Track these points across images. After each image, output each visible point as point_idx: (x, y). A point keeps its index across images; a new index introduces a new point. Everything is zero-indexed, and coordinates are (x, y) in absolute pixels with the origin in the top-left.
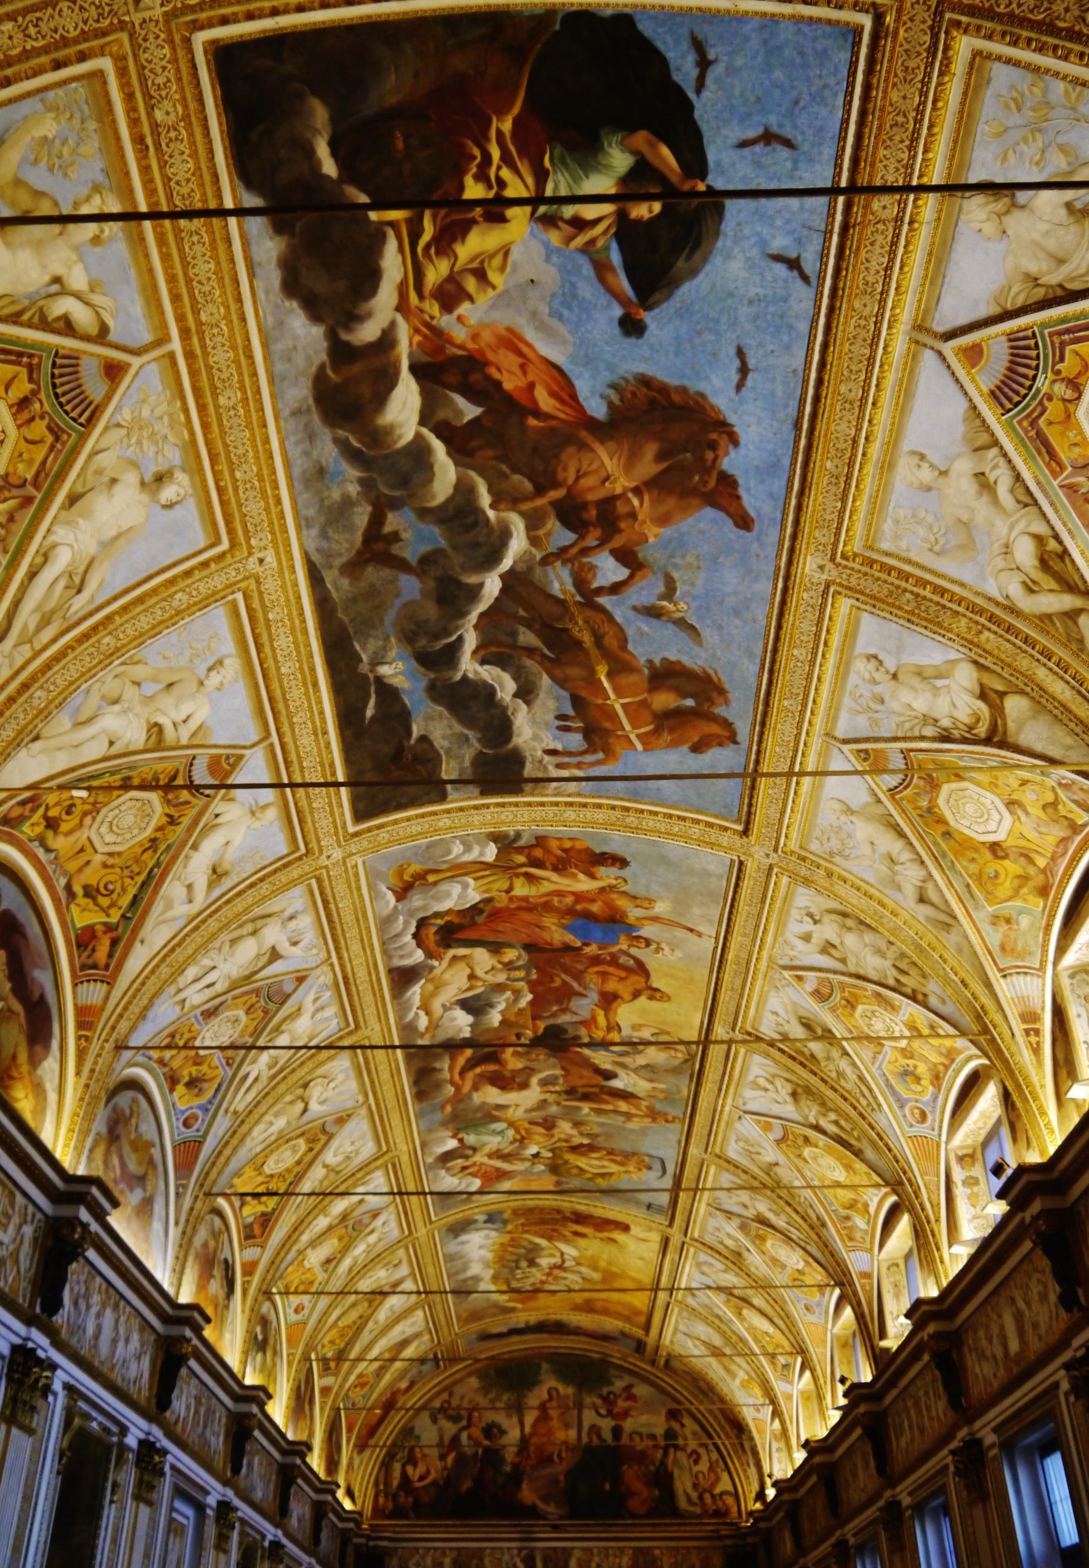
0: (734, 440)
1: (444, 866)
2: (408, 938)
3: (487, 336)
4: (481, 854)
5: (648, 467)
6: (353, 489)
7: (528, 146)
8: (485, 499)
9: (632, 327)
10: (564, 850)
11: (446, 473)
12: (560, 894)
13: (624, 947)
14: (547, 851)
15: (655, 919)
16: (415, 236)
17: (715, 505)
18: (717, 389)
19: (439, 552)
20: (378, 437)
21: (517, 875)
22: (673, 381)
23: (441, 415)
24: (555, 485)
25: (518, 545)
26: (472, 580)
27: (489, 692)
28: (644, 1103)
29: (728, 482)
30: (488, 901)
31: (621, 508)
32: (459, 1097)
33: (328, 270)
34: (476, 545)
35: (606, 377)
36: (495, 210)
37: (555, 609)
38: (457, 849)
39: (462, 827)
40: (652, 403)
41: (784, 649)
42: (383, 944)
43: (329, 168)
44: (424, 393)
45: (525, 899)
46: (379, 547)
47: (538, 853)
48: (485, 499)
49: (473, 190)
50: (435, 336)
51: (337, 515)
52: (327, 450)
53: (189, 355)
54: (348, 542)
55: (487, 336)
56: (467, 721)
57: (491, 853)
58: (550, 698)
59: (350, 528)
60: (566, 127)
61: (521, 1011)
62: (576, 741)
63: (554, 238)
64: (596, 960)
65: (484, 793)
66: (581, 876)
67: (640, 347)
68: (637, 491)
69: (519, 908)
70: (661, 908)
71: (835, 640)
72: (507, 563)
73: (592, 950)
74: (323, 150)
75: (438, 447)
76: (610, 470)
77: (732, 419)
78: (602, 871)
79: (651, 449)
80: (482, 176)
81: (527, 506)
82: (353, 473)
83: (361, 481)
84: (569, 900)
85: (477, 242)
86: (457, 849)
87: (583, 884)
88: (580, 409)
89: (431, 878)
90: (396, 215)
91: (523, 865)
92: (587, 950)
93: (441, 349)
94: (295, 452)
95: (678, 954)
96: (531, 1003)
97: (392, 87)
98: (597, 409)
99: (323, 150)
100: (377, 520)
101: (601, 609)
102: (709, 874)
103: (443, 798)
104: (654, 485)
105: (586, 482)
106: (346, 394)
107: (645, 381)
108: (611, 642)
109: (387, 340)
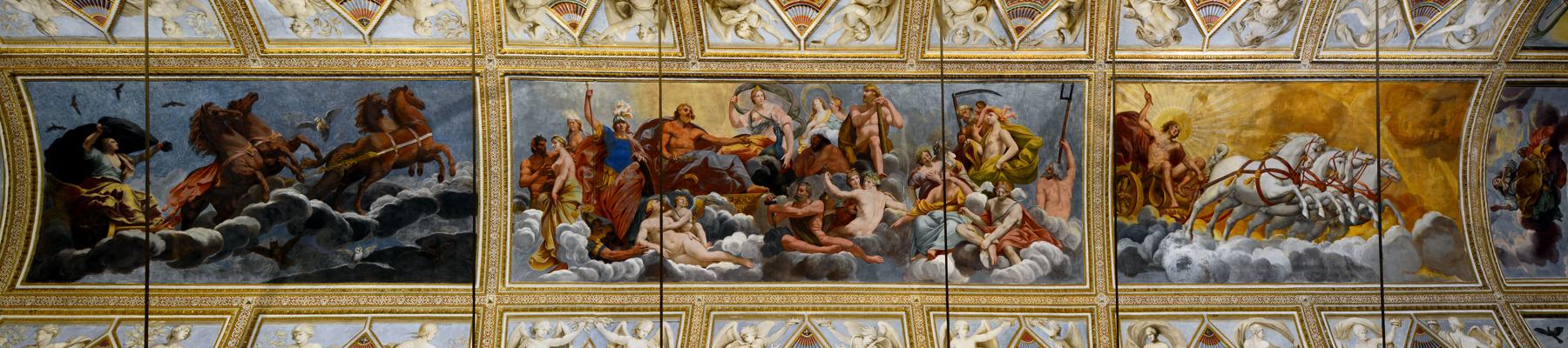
0: (210, 104)
1: (542, 239)
2: (609, 266)
3: (174, 200)
4: (534, 217)
5: (237, 138)
6: (239, 258)
7: (93, 184)
8: (262, 204)
9: (167, 147)
10: (533, 172)
11: (242, 220)
12: (579, 176)
13: (631, 137)
14: (534, 181)
15: (590, 120)
16: (123, 224)
17: (249, 110)
18: (187, 113)
19: (289, 226)
20: (214, 245)
21: (560, 199)
22: (189, 131)
23: (210, 220)
24: (255, 175)
25: (291, 192)
26: (310, 212)
27: (389, 211)
28: (855, 113)
29: (232, 105)
30: (586, 216)
31: (265, 148)
32: (863, 247)
33: (127, 257)
34: (289, 210)
35: (193, 156)
36: (119, 195)
37: (332, 177)
38: (526, 230)
39: (498, 226)
40: (202, 138)
41: (314, 71)
42: (603, 282)
43: (86, 251)
44: (197, 226)
45: (586, 196)
46: (277, 252)
47: (536, 186)
48: (262, 204)
49: (111, 202)
50: (169, 220)
51: (249, 271)
52: (213, 266)
53: (124, 313)
54: (270, 265)
55: (174, 200)
56: (411, 220)
57: (534, 215)
58: (400, 179)
59: (259, 263)
60: (89, 172)
61: (732, 200)
62: (426, 166)
63: (130, 175)
64: (654, 152)
65: (475, 212)
66: (558, 162)
67: (175, 143)
68: (253, 142)
69: (598, 198)
70: (573, 115)
71: (294, 48)
72: (302, 196)
73: (641, 156)
74: (79, 252)
75: (226, 222)
76: (243, 154)
77: (199, 106)
78: (550, 152)
79: (227, 137)
80: (103, 200)
81: (267, 188)
82: (230, 257)
83: (236, 255)
84: (584, 169)
85: (130, 203)
86: (526, 230)
87: (567, 161)
88: (211, 166)
89: (551, 246)
90: (112, 230)
91: (550, 195)
92: (640, 158)
93: (177, 219)
94: (205, 279)
95: (622, 103)
96: (721, 193)
97: (63, 227)
98: (210, 159)
99: (79, 252)
100: (262, 251)
101: (330, 156)
102: (532, 92)
103: (474, 236)
104: (248, 134)
105: (252, 162)
106: (186, 257)
107: (192, 141)
108: (351, 151)
109: (168, 239)
